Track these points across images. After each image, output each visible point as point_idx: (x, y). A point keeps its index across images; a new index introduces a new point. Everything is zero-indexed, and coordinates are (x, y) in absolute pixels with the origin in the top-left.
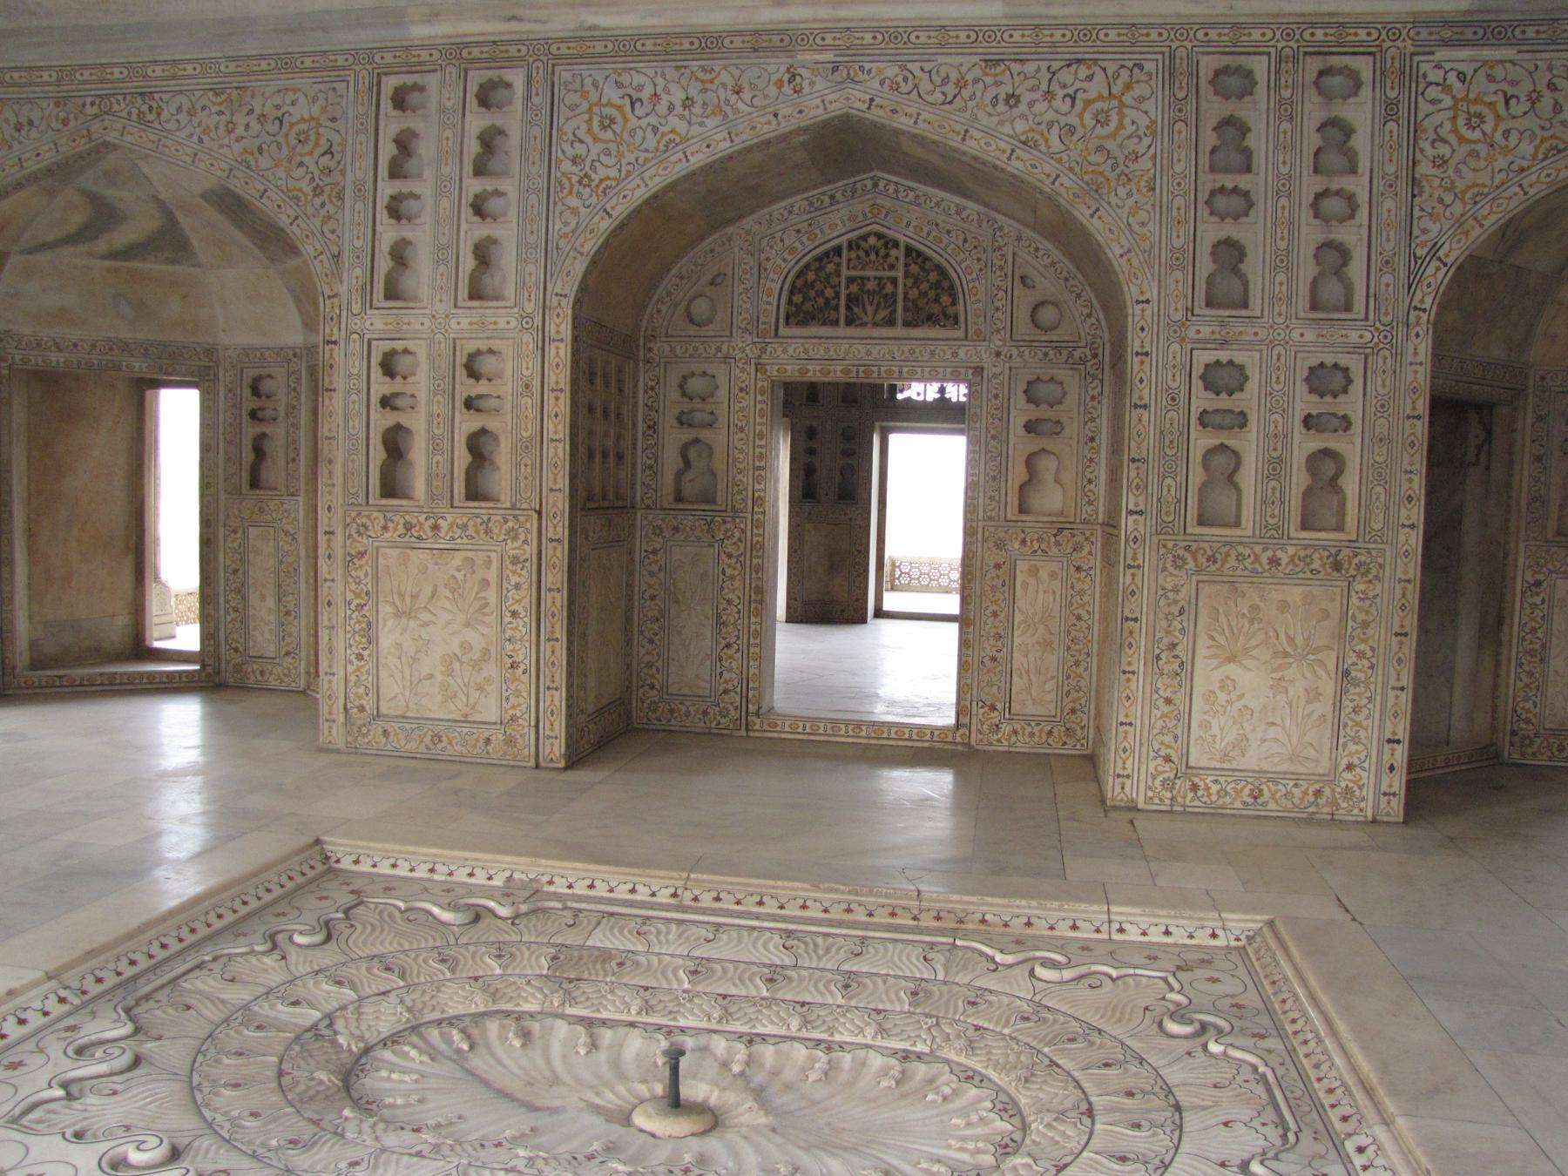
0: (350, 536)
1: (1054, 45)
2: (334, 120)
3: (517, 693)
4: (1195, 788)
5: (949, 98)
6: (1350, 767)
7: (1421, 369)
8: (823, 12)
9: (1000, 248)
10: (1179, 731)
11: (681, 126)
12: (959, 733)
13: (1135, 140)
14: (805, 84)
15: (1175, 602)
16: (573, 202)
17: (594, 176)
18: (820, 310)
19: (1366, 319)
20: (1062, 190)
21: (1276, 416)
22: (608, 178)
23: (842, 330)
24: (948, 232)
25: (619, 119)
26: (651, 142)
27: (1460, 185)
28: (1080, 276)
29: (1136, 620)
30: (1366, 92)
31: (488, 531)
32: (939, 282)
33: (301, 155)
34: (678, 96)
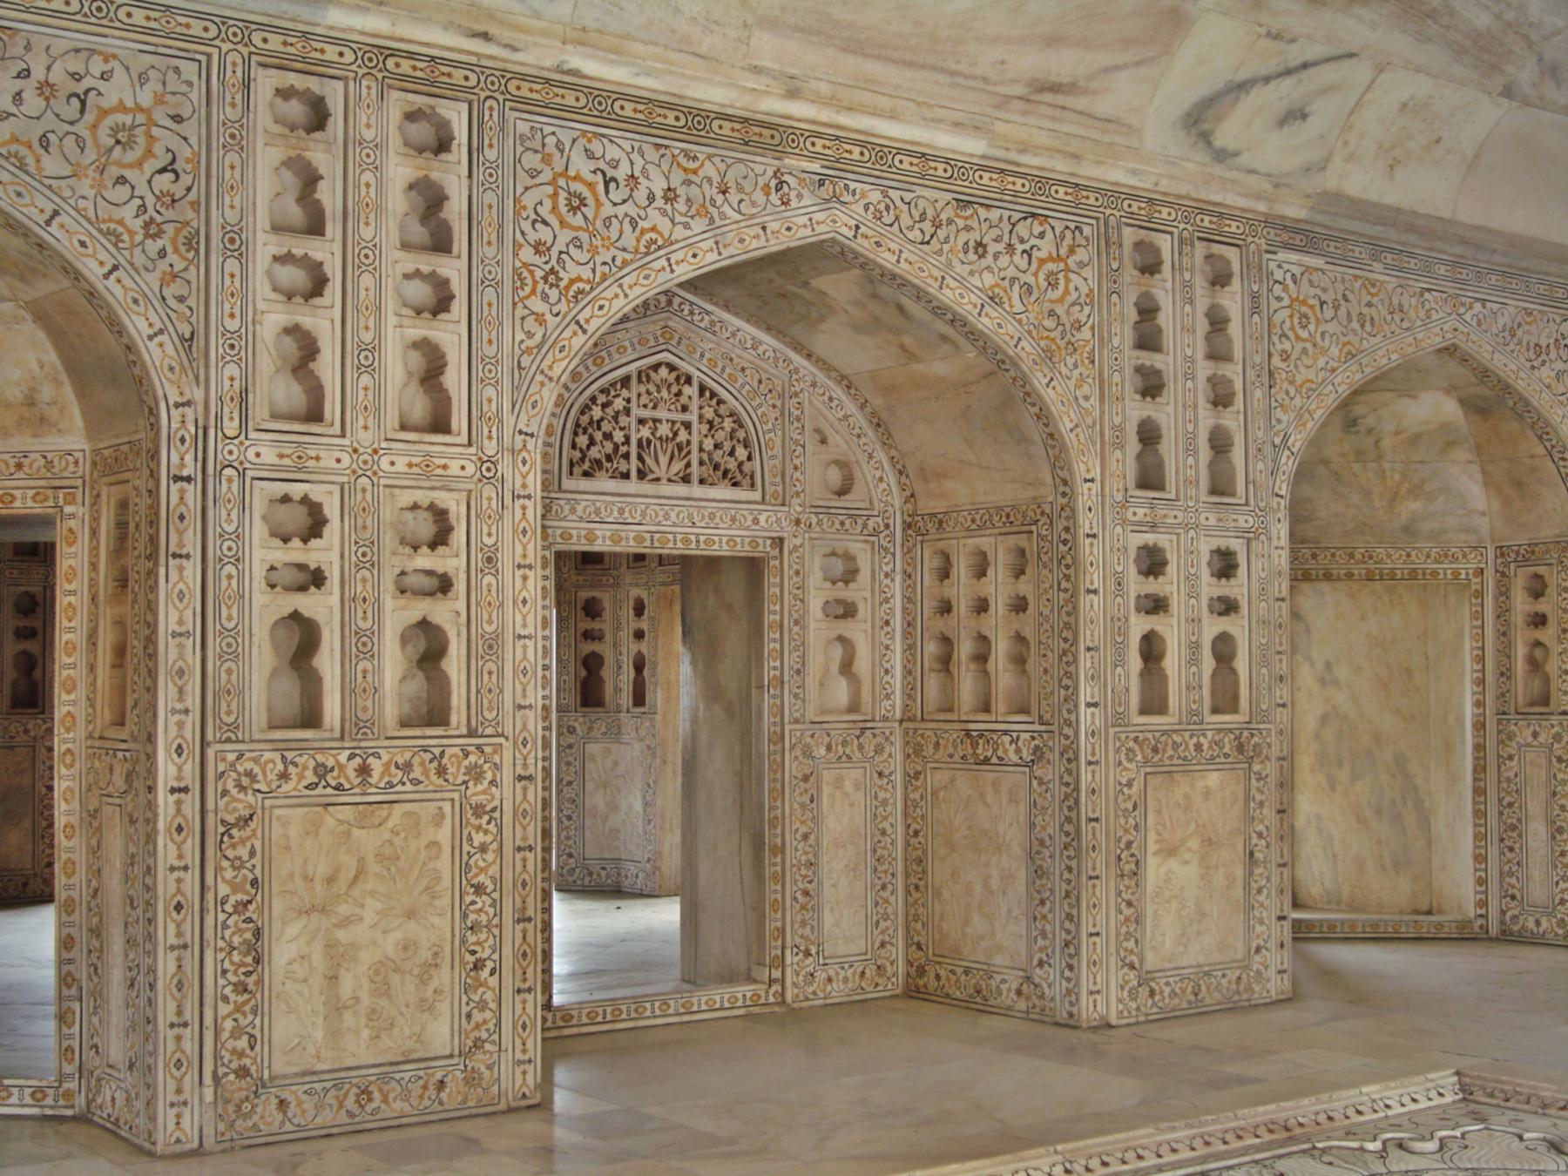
0: (225, 793)
1: (1015, 194)
2: (177, 119)
3: (482, 1005)
4: (1152, 993)
5: (927, 238)
6: (1258, 950)
7: (1283, 553)
8: (825, 115)
9: (796, 394)
10: (1138, 935)
11: (664, 225)
12: (772, 992)
13: (1078, 308)
14: (793, 194)
15: (1130, 797)
16: (537, 305)
17: (562, 274)
18: (609, 458)
19: (1247, 504)
20: (1023, 355)
21: (1193, 601)
22: (579, 279)
23: (633, 486)
24: (743, 370)
25: (590, 201)
26: (629, 239)
27: (1299, 380)
28: (870, 433)
29: (1096, 820)
30: (1236, 280)
31: (442, 771)
32: (733, 430)
33: (119, 164)
34: (659, 186)
